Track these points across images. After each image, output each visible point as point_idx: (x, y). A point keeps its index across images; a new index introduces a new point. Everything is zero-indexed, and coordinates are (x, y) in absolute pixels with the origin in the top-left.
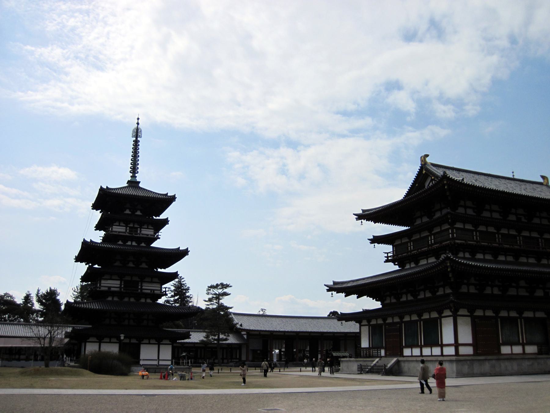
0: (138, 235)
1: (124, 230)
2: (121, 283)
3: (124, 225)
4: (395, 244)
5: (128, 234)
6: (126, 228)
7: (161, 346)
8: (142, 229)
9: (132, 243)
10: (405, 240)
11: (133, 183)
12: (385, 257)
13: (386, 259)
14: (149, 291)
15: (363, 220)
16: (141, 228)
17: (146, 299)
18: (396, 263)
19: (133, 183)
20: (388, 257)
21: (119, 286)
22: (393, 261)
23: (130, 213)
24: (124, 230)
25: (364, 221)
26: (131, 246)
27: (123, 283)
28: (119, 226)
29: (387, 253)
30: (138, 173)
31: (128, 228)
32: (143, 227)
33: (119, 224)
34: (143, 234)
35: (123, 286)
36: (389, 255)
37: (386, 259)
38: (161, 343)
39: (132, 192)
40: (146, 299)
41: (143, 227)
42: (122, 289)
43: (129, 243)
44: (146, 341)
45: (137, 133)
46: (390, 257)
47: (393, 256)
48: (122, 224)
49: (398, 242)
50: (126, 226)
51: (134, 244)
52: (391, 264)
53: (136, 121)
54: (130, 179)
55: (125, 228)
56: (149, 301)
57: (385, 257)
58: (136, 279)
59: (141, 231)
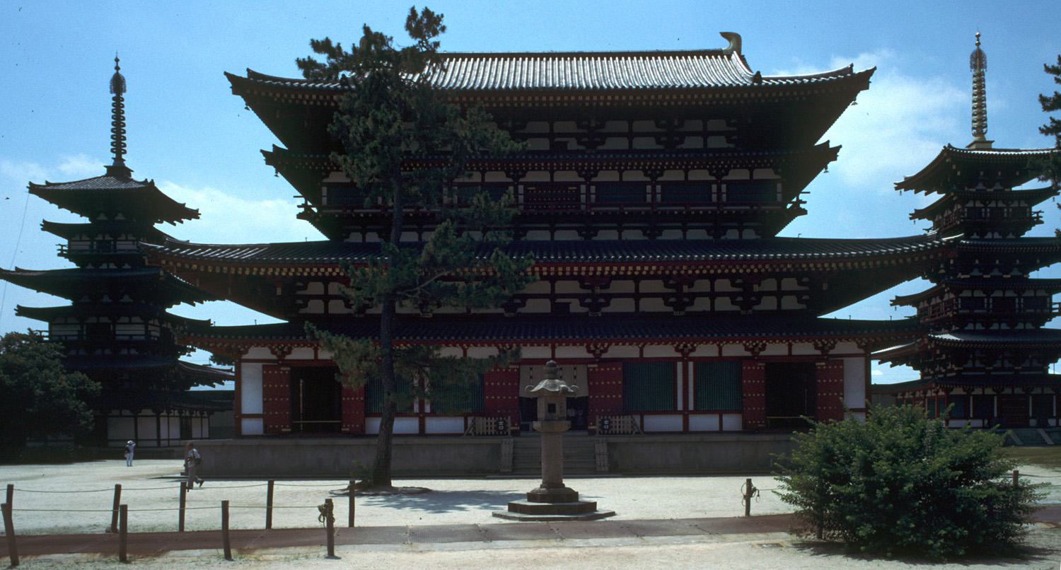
0: (112, 253)
1: (87, 248)
2: (82, 328)
3: (88, 239)
5: (95, 253)
6: (92, 243)
7: (139, 419)
8: (118, 243)
9: (108, 266)
11: (119, 170)
14: (127, 338)
16: (115, 241)
19: (119, 170)
21: (77, 333)
23: (105, 218)
24: (87, 248)
26: (108, 270)
27: (85, 329)
28: (81, 241)
30: (125, 152)
31: (95, 243)
32: (119, 239)
33: (81, 237)
34: (120, 250)
35: (85, 333)
38: (140, 414)
39: (113, 184)
41: (119, 239)
42: (85, 338)
43: (104, 266)
44: (115, 412)
48: (85, 238)
50: (92, 241)
51: (112, 266)
53: (114, 64)
54: (111, 163)
55: (89, 243)
58: (105, 320)
59: (115, 246)
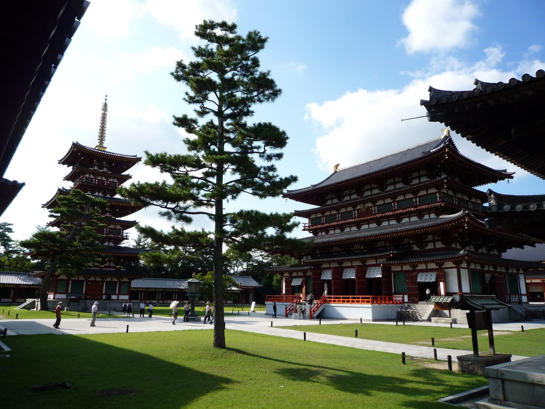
4: (311, 218)
10: (319, 215)
12: (303, 227)
13: (304, 228)
15: (287, 198)
17: (109, 242)
18: (311, 232)
20: (305, 227)
22: (309, 230)
25: (288, 199)
29: (305, 224)
36: (306, 225)
37: (304, 228)
40: (109, 242)
45: (106, 105)
46: (307, 227)
47: (309, 226)
49: (313, 216)
52: (307, 232)
56: (111, 244)
57: (303, 227)
